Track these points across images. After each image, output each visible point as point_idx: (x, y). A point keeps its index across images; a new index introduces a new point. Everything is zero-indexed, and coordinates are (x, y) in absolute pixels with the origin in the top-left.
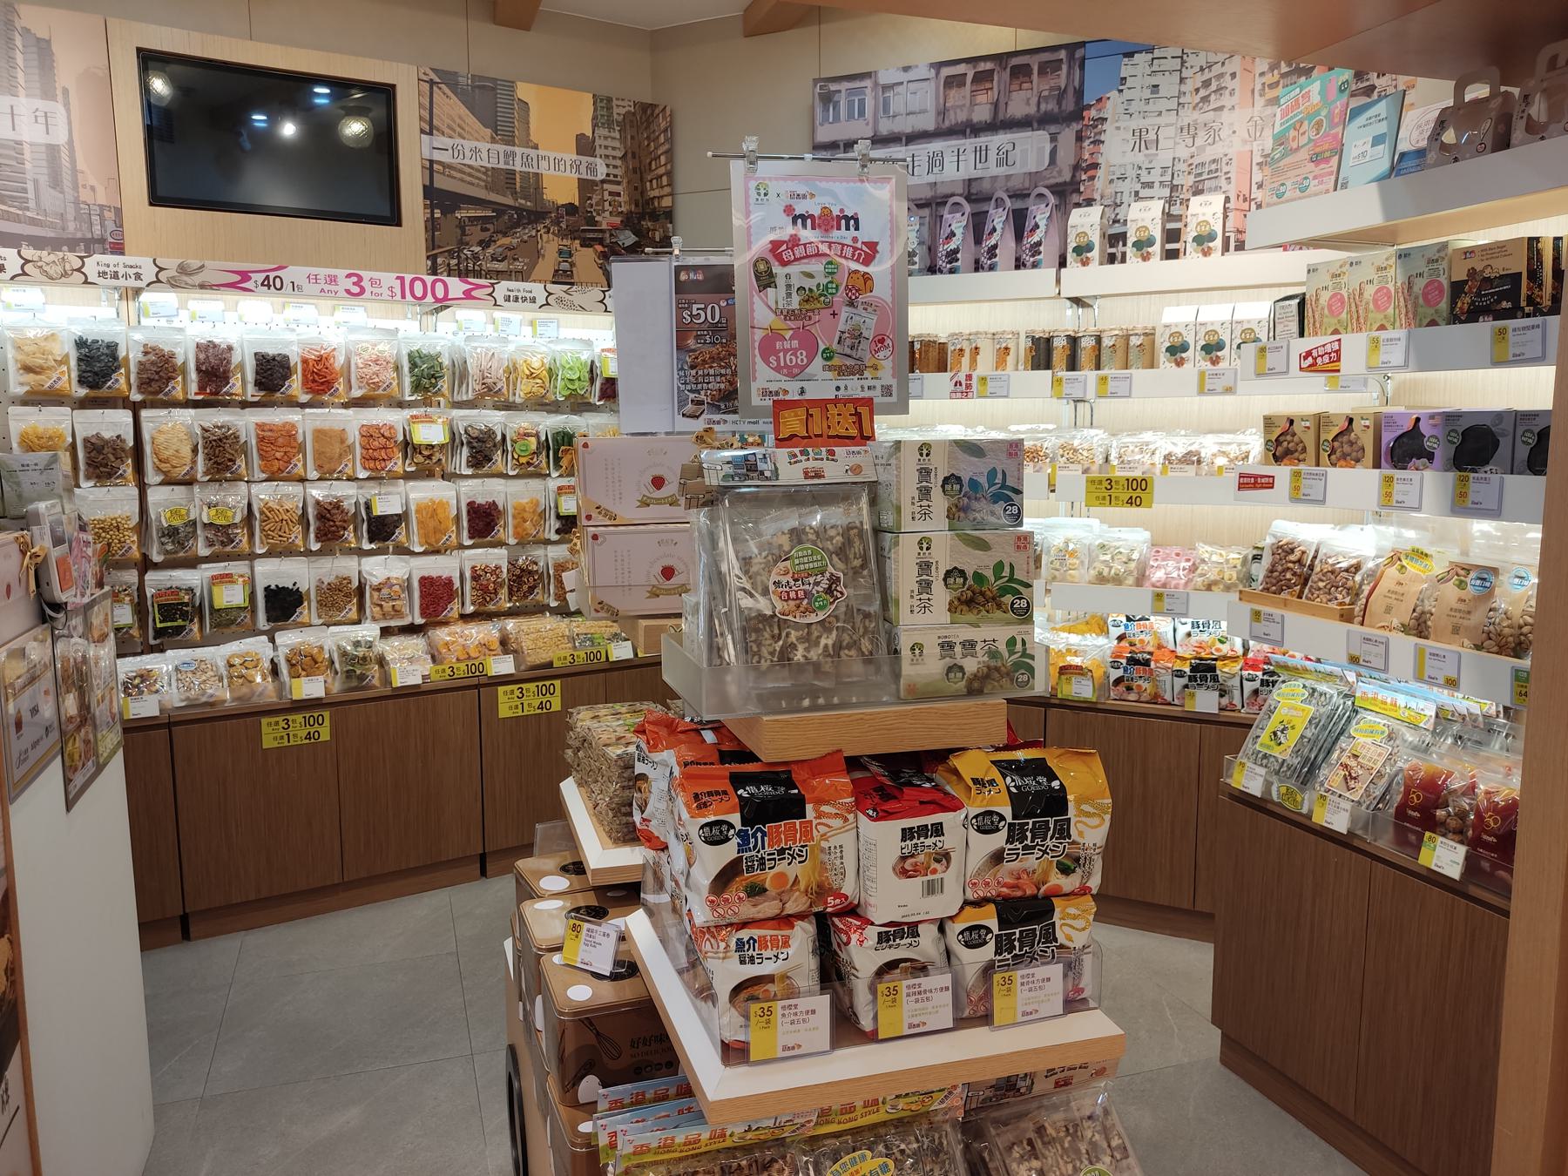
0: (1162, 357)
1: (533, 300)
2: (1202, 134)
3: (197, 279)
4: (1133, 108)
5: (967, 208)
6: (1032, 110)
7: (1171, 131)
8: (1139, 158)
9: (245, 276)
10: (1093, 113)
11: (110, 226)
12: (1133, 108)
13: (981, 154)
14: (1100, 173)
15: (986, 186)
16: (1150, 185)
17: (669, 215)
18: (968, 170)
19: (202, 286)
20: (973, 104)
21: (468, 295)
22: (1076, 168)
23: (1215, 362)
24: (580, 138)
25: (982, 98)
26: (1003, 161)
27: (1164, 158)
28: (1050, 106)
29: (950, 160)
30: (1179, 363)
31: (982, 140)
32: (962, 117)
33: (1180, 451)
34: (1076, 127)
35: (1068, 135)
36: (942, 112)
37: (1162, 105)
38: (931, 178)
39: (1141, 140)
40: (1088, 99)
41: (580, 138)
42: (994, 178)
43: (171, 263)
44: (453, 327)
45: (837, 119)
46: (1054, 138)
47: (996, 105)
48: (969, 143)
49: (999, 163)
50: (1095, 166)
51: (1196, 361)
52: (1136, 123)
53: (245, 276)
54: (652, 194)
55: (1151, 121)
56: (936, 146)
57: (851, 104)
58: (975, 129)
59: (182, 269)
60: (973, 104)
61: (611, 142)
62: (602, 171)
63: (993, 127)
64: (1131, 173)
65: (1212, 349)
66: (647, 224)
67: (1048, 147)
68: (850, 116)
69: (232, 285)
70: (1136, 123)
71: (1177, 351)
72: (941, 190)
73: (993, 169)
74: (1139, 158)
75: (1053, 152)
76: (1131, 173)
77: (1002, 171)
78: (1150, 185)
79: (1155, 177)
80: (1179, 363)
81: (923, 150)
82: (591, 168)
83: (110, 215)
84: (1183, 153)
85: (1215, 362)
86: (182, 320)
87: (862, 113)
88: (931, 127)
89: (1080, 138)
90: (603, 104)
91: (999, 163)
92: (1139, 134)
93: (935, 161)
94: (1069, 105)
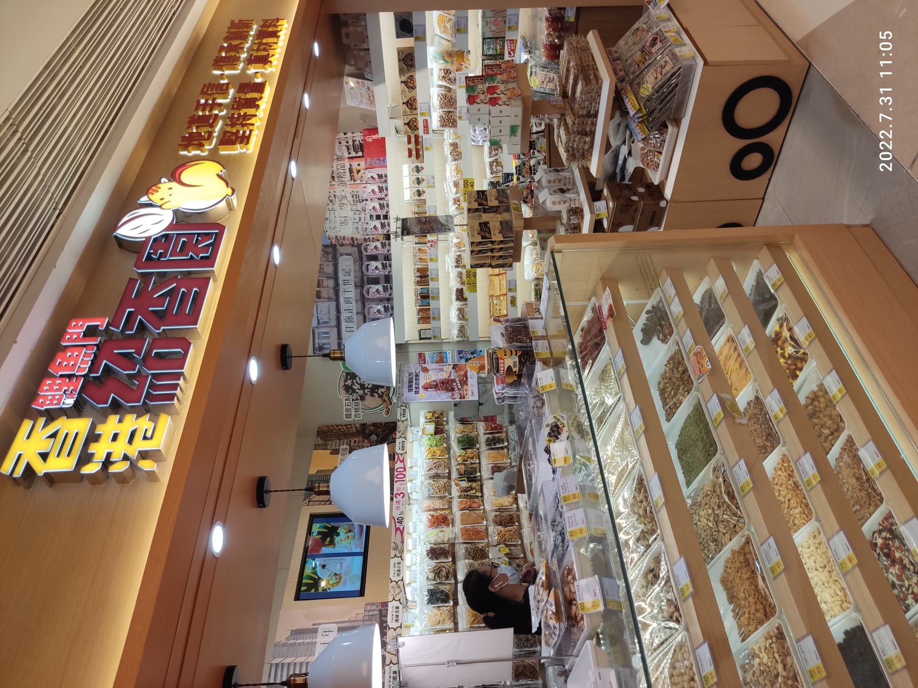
0: (422, 198)
1: (399, 563)
2: (343, 202)
3: (400, 545)
4: (332, 226)
5: (367, 287)
6: (331, 264)
7: (342, 212)
8: (350, 223)
9: (397, 529)
10: (334, 241)
11: (374, 607)
12: (332, 226)
13: (346, 282)
14: (355, 236)
15: (358, 280)
16: (360, 218)
17: (363, 425)
18: (351, 287)
19: (403, 542)
20: (327, 287)
21: (402, 461)
22: (353, 245)
23: (423, 180)
24: (331, 453)
25: (325, 284)
26: (349, 274)
27: (351, 214)
28: (330, 256)
29: (348, 295)
30: (424, 192)
31: (341, 282)
32: (332, 291)
33: (456, 304)
34: (338, 247)
35: (341, 250)
36: (329, 299)
37: (332, 216)
38: (354, 302)
39: (344, 223)
40: (328, 243)
41: (331, 453)
42: (355, 277)
43: (393, 553)
44: (414, 494)
45: (329, 344)
46: (342, 255)
47: (328, 278)
48: (342, 287)
49: (349, 275)
50: (352, 238)
51: (422, 187)
52: (338, 225)
53: (397, 529)
54: (354, 430)
55: (338, 220)
56: (342, 301)
57: (324, 338)
58: (337, 285)
59: (396, 549)
60: (327, 287)
61: (334, 444)
62: (345, 446)
63: (336, 277)
64: (356, 225)
65: (419, 181)
66: (367, 431)
67: (345, 257)
68: (328, 338)
69: (402, 533)
70: (338, 225)
71: (419, 193)
72: (359, 298)
73: (352, 277)
74: (350, 223)
75: (347, 254)
76: (356, 225)
77: (352, 274)
78: (360, 218)
79: (357, 217)
80: (424, 192)
81: (343, 306)
82: (344, 450)
83: (369, 608)
84: (349, 207)
85: (423, 180)
86: (417, 585)
87: (327, 333)
88: (334, 304)
89: (342, 245)
90: (317, 447)
91: (349, 275)
92: (342, 223)
93: (348, 301)
94: (330, 250)
